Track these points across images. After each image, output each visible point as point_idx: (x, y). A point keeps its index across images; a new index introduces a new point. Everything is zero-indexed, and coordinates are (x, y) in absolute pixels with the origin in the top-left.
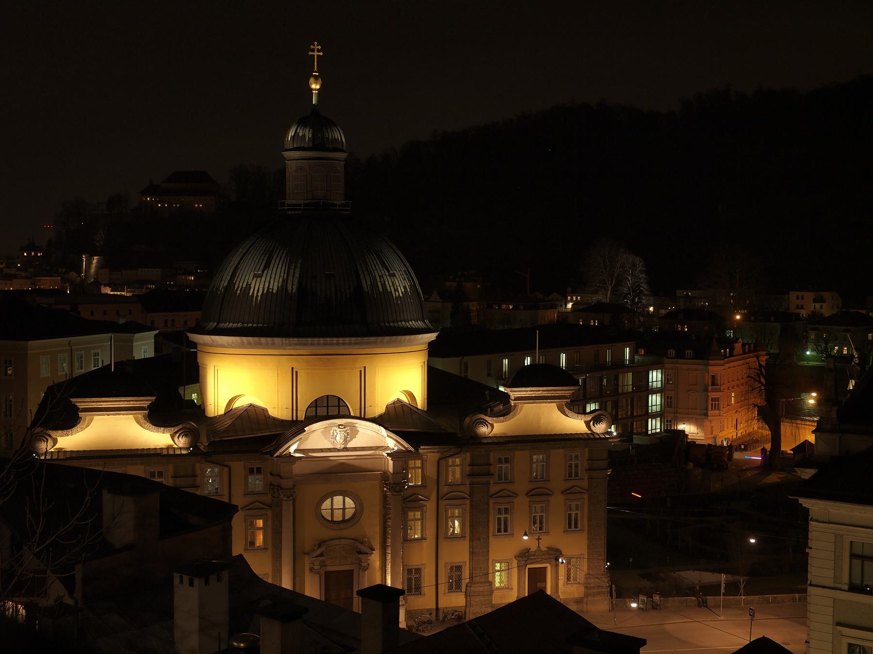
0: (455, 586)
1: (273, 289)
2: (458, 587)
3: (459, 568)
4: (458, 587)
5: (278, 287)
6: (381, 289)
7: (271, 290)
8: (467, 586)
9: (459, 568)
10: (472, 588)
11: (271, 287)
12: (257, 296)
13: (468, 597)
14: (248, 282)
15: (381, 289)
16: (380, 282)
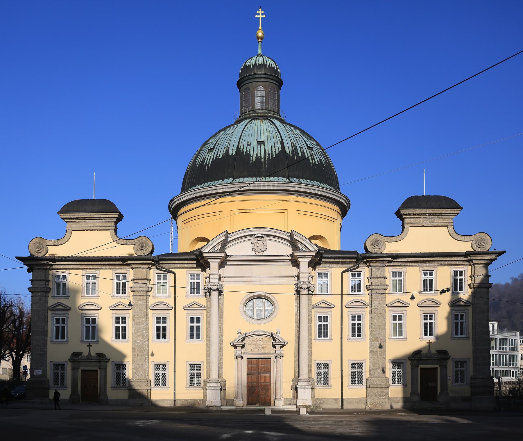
0: (357, 379)
1: (219, 156)
2: (360, 382)
3: (360, 365)
4: (360, 382)
5: (223, 154)
6: (300, 155)
7: (218, 157)
8: (367, 380)
9: (360, 365)
10: (371, 381)
11: (218, 155)
12: (209, 163)
13: (368, 389)
14: (204, 157)
15: (300, 155)
16: (300, 150)
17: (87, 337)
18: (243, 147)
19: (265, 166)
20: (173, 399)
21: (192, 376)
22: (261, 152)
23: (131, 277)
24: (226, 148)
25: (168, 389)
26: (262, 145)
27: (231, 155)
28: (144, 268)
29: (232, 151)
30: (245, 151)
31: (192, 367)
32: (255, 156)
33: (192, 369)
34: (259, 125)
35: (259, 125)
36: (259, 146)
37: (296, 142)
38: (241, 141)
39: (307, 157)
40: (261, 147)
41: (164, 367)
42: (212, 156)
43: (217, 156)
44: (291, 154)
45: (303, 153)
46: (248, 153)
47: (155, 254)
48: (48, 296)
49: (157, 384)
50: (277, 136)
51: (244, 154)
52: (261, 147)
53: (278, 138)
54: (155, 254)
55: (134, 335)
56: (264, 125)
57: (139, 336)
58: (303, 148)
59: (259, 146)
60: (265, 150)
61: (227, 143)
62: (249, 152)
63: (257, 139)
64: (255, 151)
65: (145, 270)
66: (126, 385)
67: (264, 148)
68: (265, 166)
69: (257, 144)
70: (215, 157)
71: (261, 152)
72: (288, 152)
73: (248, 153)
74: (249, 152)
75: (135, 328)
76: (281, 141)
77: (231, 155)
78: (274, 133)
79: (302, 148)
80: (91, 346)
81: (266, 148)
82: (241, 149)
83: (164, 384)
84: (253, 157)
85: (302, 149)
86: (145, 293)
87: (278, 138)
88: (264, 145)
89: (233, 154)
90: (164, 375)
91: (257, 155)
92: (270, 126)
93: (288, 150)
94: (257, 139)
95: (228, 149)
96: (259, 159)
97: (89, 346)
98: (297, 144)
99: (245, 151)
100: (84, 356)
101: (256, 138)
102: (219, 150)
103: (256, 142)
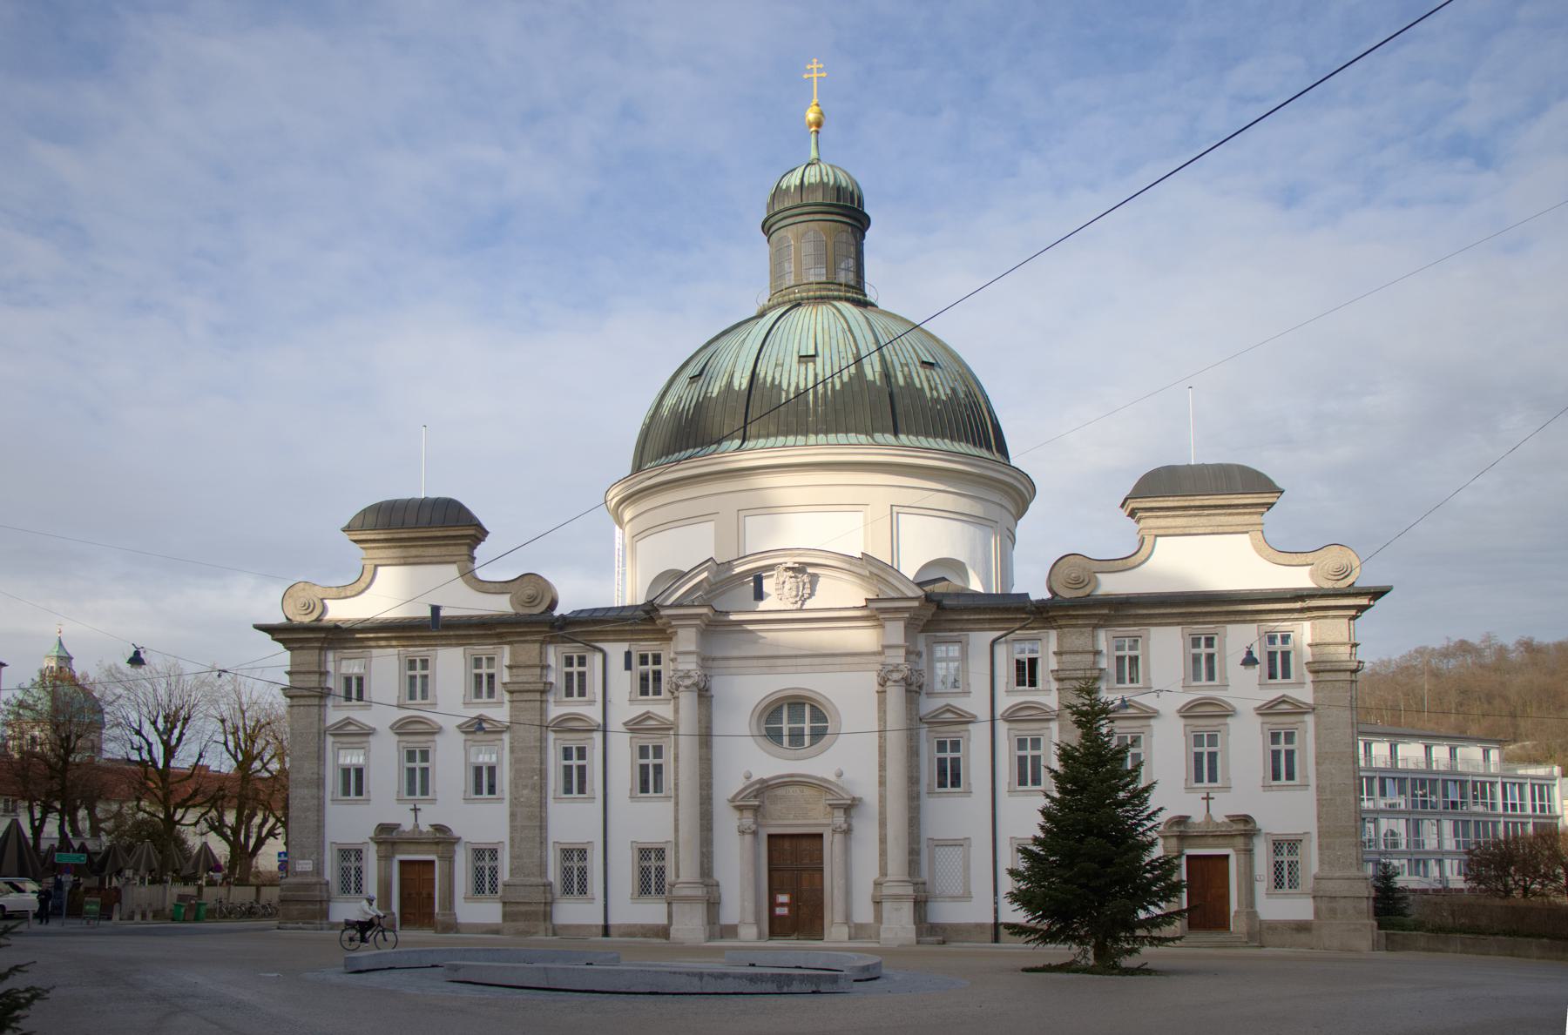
1: (712, 393)
5: (720, 387)
6: (901, 381)
7: (709, 395)
11: (710, 390)
15: (901, 381)
16: (902, 371)
17: (411, 792)
18: (766, 371)
19: (816, 411)
20: (601, 922)
21: (644, 873)
22: (806, 379)
23: (507, 661)
24: (727, 375)
25: (591, 901)
26: (811, 365)
27: (737, 388)
28: (534, 642)
29: (741, 382)
30: (769, 379)
31: (644, 853)
32: (792, 389)
33: (645, 859)
34: (807, 319)
35: (807, 319)
36: (803, 367)
37: (893, 353)
38: (761, 356)
39: (918, 385)
40: (806, 369)
41: (582, 853)
42: (697, 393)
43: (706, 393)
44: (878, 383)
45: (909, 378)
46: (777, 382)
47: (557, 613)
48: (326, 705)
49: (568, 889)
50: (847, 342)
51: (768, 385)
52: (806, 369)
53: (848, 346)
54: (557, 613)
55: (514, 784)
56: (819, 318)
57: (525, 787)
58: (908, 367)
59: (803, 367)
60: (816, 375)
61: (730, 364)
62: (780, 382)
63: (799, 352)
64: (793, 378)
65: (537, 646)
66: (496, 892)
67: (815, 369)
68: (816, 411)
69: (799, 362)
70: (702, 395)
71: (806, 379)
72: (870, 377)
73: (777, 382)
74: (780, 382)
75: (516, 770)
76: (855, 352)
77: (737, 388)
78: (840, 334)
79: (907, 365)
80: (419, 809)
81: (819, 371)
82: (762, 375)
83: (583, 890)
84: (788, 392)
85: (906, 369)
86: (538, 696)
87: (848, 346)
88: (815, 364)
89: (743, 387)
90: (583, 872)
91: (797, 387)
92: (832, 321)
93: (872, 370)
94: (799, 352)
95: (732, 376)
96: (800, 395)
97: (416, 810)
98: (895, 358)
99: (769, 379)
100: (404, 831)
101: (796, 349)
102: (711, 378)
103: (795, 358)
